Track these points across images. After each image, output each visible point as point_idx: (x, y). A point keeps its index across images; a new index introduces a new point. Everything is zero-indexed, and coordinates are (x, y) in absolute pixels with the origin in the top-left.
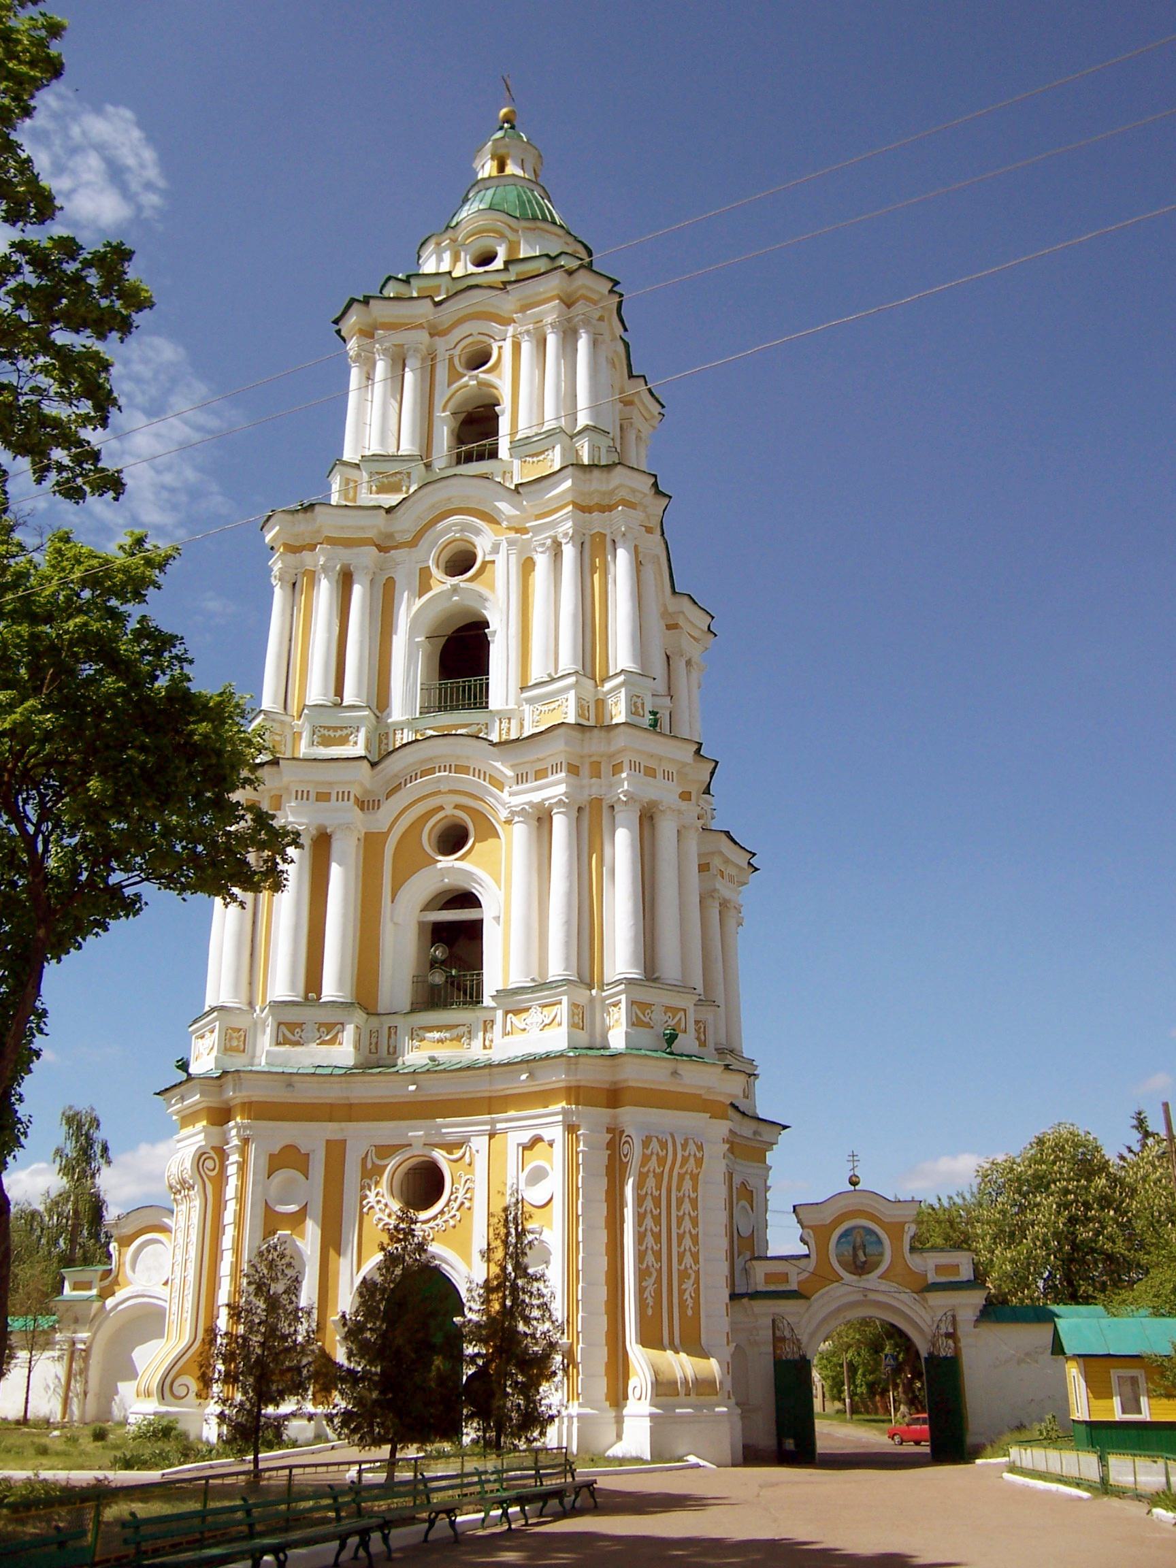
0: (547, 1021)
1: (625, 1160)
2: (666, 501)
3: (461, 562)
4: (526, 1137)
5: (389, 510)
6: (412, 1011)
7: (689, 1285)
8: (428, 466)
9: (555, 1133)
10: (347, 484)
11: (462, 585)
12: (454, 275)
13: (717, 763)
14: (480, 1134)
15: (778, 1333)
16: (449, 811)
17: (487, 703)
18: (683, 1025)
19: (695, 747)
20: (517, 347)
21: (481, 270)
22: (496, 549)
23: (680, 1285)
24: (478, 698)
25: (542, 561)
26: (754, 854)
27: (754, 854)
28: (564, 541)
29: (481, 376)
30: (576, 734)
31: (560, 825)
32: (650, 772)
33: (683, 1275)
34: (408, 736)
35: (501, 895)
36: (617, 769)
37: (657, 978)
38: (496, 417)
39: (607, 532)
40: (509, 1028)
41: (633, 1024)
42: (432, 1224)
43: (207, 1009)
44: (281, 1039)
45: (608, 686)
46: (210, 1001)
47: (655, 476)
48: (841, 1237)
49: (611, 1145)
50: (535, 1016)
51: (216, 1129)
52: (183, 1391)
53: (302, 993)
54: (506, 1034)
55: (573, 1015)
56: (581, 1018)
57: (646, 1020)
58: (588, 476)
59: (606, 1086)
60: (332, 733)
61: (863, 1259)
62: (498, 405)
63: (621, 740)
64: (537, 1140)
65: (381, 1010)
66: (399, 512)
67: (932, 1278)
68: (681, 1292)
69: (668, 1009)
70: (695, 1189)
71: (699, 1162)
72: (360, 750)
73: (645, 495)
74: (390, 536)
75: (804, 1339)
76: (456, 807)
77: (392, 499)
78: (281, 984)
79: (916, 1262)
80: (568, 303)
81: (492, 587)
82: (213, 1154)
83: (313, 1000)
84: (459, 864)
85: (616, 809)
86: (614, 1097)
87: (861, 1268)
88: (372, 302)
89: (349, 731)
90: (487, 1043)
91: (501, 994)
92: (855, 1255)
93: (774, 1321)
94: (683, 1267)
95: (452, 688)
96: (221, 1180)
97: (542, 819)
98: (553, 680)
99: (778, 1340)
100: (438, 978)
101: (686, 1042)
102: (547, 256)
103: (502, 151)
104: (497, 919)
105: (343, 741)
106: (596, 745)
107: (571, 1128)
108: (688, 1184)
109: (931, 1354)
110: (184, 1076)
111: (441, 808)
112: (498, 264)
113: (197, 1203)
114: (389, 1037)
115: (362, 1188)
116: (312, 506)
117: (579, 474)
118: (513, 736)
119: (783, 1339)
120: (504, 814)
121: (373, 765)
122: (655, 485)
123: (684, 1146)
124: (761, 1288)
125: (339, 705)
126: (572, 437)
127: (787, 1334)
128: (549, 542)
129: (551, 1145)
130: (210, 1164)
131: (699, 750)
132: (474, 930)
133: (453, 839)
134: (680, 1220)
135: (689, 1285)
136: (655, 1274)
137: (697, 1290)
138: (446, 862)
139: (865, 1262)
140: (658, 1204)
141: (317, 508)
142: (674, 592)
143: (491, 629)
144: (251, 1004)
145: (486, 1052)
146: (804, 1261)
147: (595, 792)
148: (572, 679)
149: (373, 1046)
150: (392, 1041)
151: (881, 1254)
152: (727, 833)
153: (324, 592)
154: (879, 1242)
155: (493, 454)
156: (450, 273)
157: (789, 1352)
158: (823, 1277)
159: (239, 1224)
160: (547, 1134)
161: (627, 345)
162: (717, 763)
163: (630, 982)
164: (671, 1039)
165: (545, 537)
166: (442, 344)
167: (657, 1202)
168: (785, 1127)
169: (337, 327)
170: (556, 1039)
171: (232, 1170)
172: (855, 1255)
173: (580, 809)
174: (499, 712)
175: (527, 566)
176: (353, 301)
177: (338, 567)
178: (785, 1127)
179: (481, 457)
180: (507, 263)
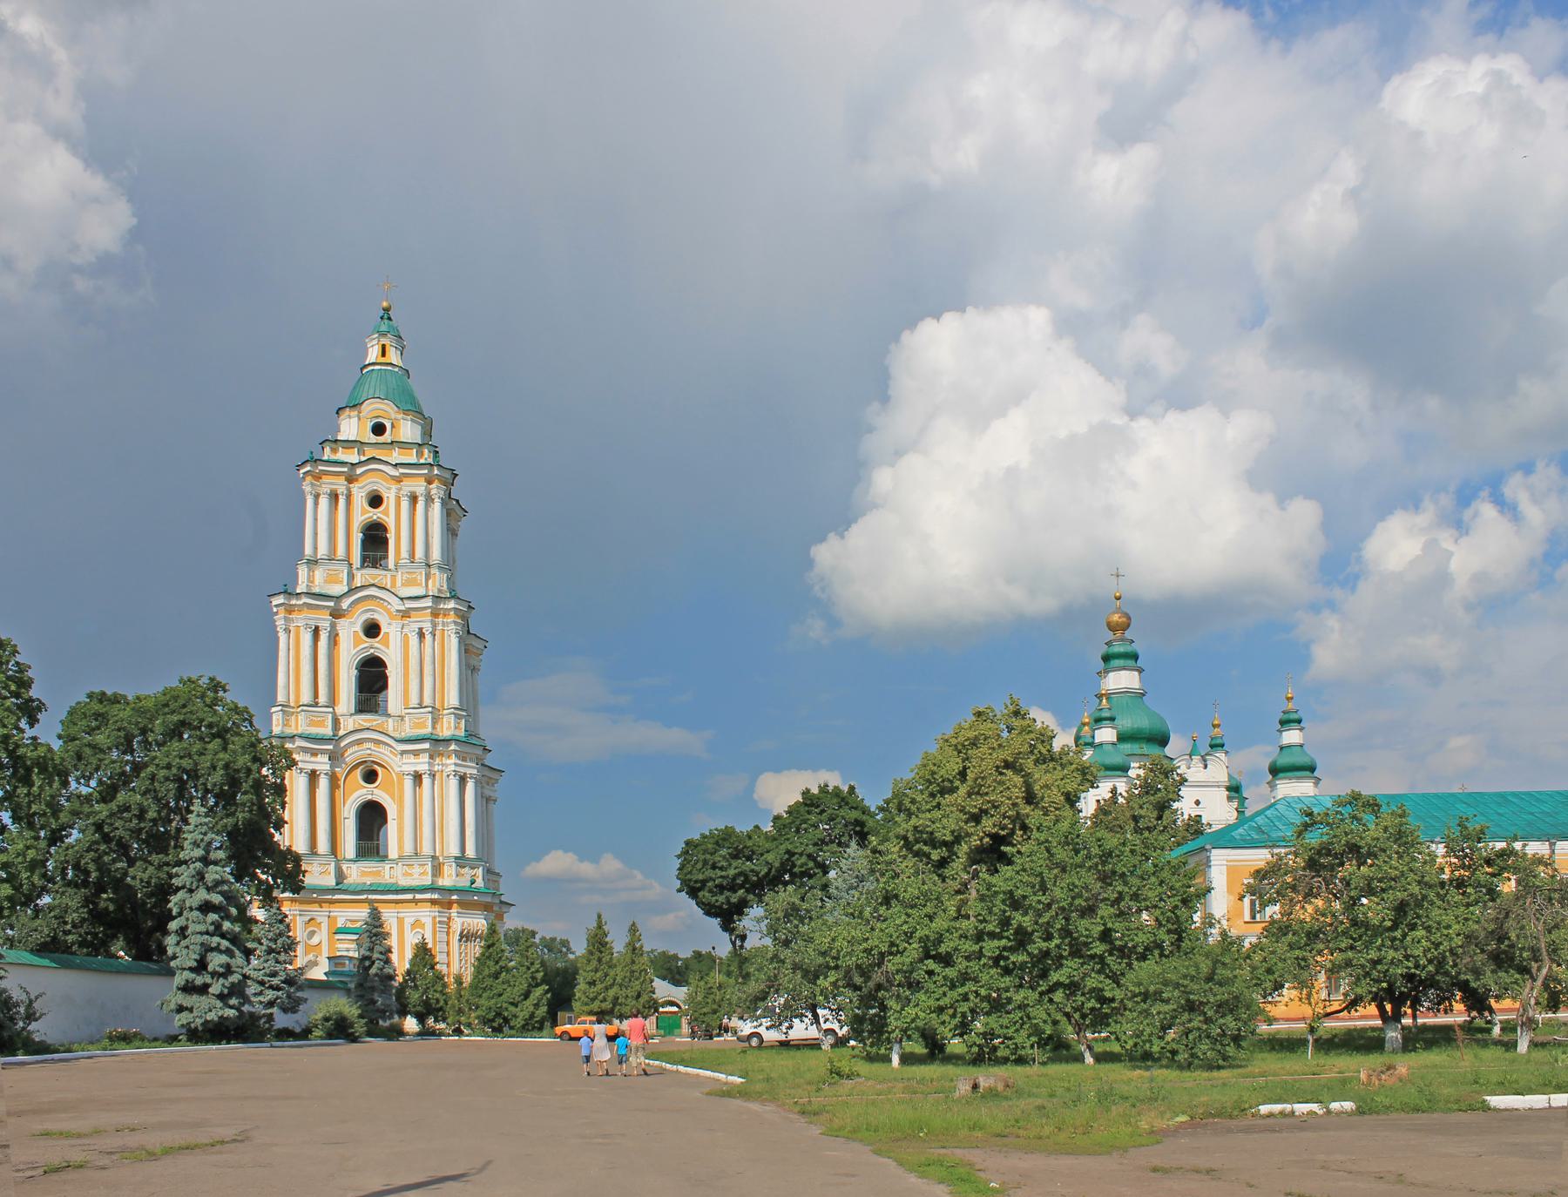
3: (372, 630)
4: (412, 920)
20: (398, 499)
25: (414, 640)
31: (426, 780)
50: (417, 870)
56: (437, 870)
63: (453, 747)
86: (449, 905)
97: (418, 778)
105: (321, 724)
112: (387, 437)
120: (398, 770)
125: (316, 705)
133: (371, 776)
160: (423, 920)
165: (416, 627)
166: (355, 488)
170: (427, 881)
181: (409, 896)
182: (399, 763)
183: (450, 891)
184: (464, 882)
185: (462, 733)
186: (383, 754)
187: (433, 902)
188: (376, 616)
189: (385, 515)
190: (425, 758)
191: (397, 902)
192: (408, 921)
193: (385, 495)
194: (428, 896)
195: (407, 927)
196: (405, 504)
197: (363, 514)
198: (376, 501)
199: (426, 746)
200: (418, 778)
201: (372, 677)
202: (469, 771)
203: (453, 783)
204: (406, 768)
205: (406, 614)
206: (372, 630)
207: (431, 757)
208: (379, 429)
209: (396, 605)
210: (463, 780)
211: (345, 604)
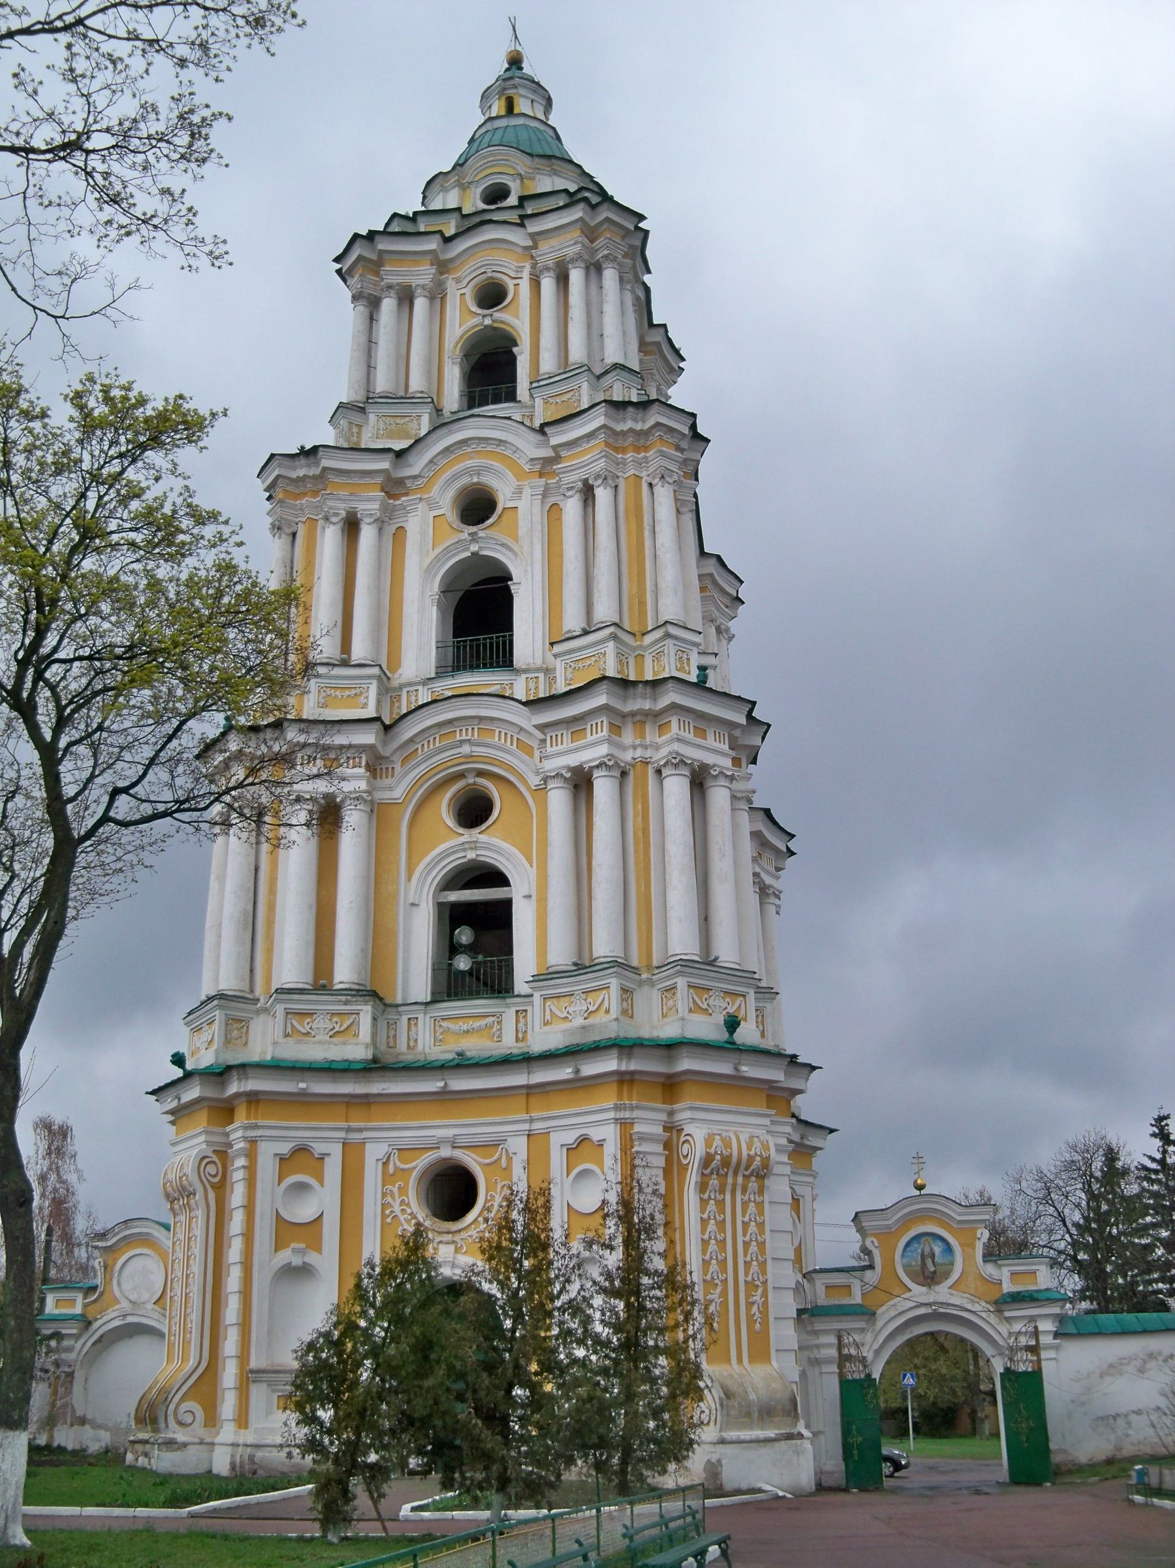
0: (591, 1009)
1: (685, 1162)
2: (705, 444)
3: (477, 507)
4: (570, 1137)
5: (400, 454)
6: (434, 1001)
7: (757, 1297)
8: (439, 411)
9: (608, 1134)
10: (350, 429)
11: (481, 534)
12: (465, 212)
13: (769, 726)
14: (516, 1134)
15: (846, 1351)
16: (471, 781)
17: (511, 661)
18: (743, 1011)
19: (747, 708)
21: (493, 207)
22: (519, 492)
23: (747, 1298)
24: (503, 657)
25: (572, 507)
26: (793, 836)
27: (793, 836)
28: (596, 484)
29: (497, 315)
30: (619, 691)
31: (603, 788)
32: (701, 732)
33: (751, 1286)
34: (424, 696)
35: (533, 872)
36: (663, 728)
37: (716, 959)
38: (512, 361)
39: (644, 474)
40: (548, 1017)
41: (690, 1011)
42: (464, 1235)
43: (204, 998)
44: (289, 1030)
45: (648, 639)
46: (207, 990)
47: (694, 415)
48: (908, 1245)
49: (667, 1145)
51: (220, 1130)
52: (188, 1418)
53: (310, 979)
54: (546, 1023)
55: (623, 1000)
57: (705, 1006)
58: (621, 414)
59: (661, 1080)
60: (338, 693)
61: (932, 1269)
62: (517, 345)
63: (671, 696)
64: (584, 1140)
65: (399, 1001)
66: (411, 457)
67: (1007, 1287)
68: (750, 1304)
69: (727, 993)
70: (761, 1191)
71: (766, 1163)
72: (370, 712)
73: (684, 435)
74: (401, 482)
75: (870, 1357)
76: (481, 773)
77: (398, 445)
78: (290, 965)
79: (990, 1270)
80: (591, 234)
81: (516, 539)
82: (215, 1158)
83: (324, 987)
84: (483, 838)
85: (665, 772)
87: (929, 1278)
88: (377, 238)
89: (358, 691)
90: (520, 1035)
91: (538, 978)
92: (924, 1265)
93: (839, 1338)
94: (749, 1278)
95: (471, 647)
96: (221, 1187)
97: (580, 783)
98: (586, 633)
99: (844, 1359)
100: (463, 963)
101: (747, 1034)
102: (566, 191)
103: (510, 92)
104: (529, 897)
106: (639, 703)
107: (625, 1125)
108: (753, 1185)
109: (1007, 1369)
110: (179, 1073)
111: (461, 775)
112: (512, 200)
113: (200, 1213)
114: (409, 1029)
115: (384, 1195)
116: (315, 449)
117: (612, 411)
118: (541, 695)
119: (849, 1357)
120: (534, 781)
121: (387, 728)
122: (693, 427)
123: (750, 1146)
124: (822, 1300)
126: (599, 377)
127: (853, 1352)
128: (580, 484)
129: (600, 1145)
130: (211, 1169)
131: (751, 710)
132: (504, 909)
133: (474, 811)
134: (745, 1225)
135: (757, 1297)
136: (719, 1289)
137: (766, 1303)
138: (468, 835)
139: (935, 1272)
140: (722, 1210)
141: (321, 453)
142: (702, 553)
143: (515, 580)
144: (252, 991)
145: (521, 1044)
146: (868, 1273)
147: (639, 753)
148: (612, 629)
149: (391, 1040)
150: (412, 1034)
151: (952, 1264)
152: (767, 812)
153: (330, 540)
154: (949, 1249)
155: (511, 396)
156: (459, 209)
157: (855, 1372)
158: (887, 1290)
159: (248, 1236)
160: (596, 1134)
161: (647, 290)
162: (769, 726)
163: (685, 965)
164: (732, 1024)
165: (575, 477)
167: (721, 1204)
168: (832, 1131)
169: (338, 266)
171: (238, 1175)
172: (924, 1265)
173: (624, 774)
174: (525, 671)
175: (554, 513)
176: (356, 236)
177: (343, 514)
178: (832, 1131)
179: (497, 400)
180: (523, 199)
181: (564, 1072)
182: (533, 760)
183: (671, 1047)
184: (707, 1028)
185: (693, 678)
186: (500, 751)
187: (625, 1080)
188: (491, 481)
189: (515, 318)
190: (600, 730)
191: (530, 1090)
192: (561, 1139)
193: (510, 284)
194: (609, 1064)
195: (557, 1159)
196: (548, 284)
197: (462, 320)
198: (492, 296)
199: (600, 698)
200: (580, 783)
201: (480, 614)
202: (709, 759)
203: (677, 788)
204: (551, 765)
205: (546, 467)
206: (477, 507)
207: (615, 729)
208: (496, 195)
209: (529, 447)
210: (699, 780)
211: (417, 464)
